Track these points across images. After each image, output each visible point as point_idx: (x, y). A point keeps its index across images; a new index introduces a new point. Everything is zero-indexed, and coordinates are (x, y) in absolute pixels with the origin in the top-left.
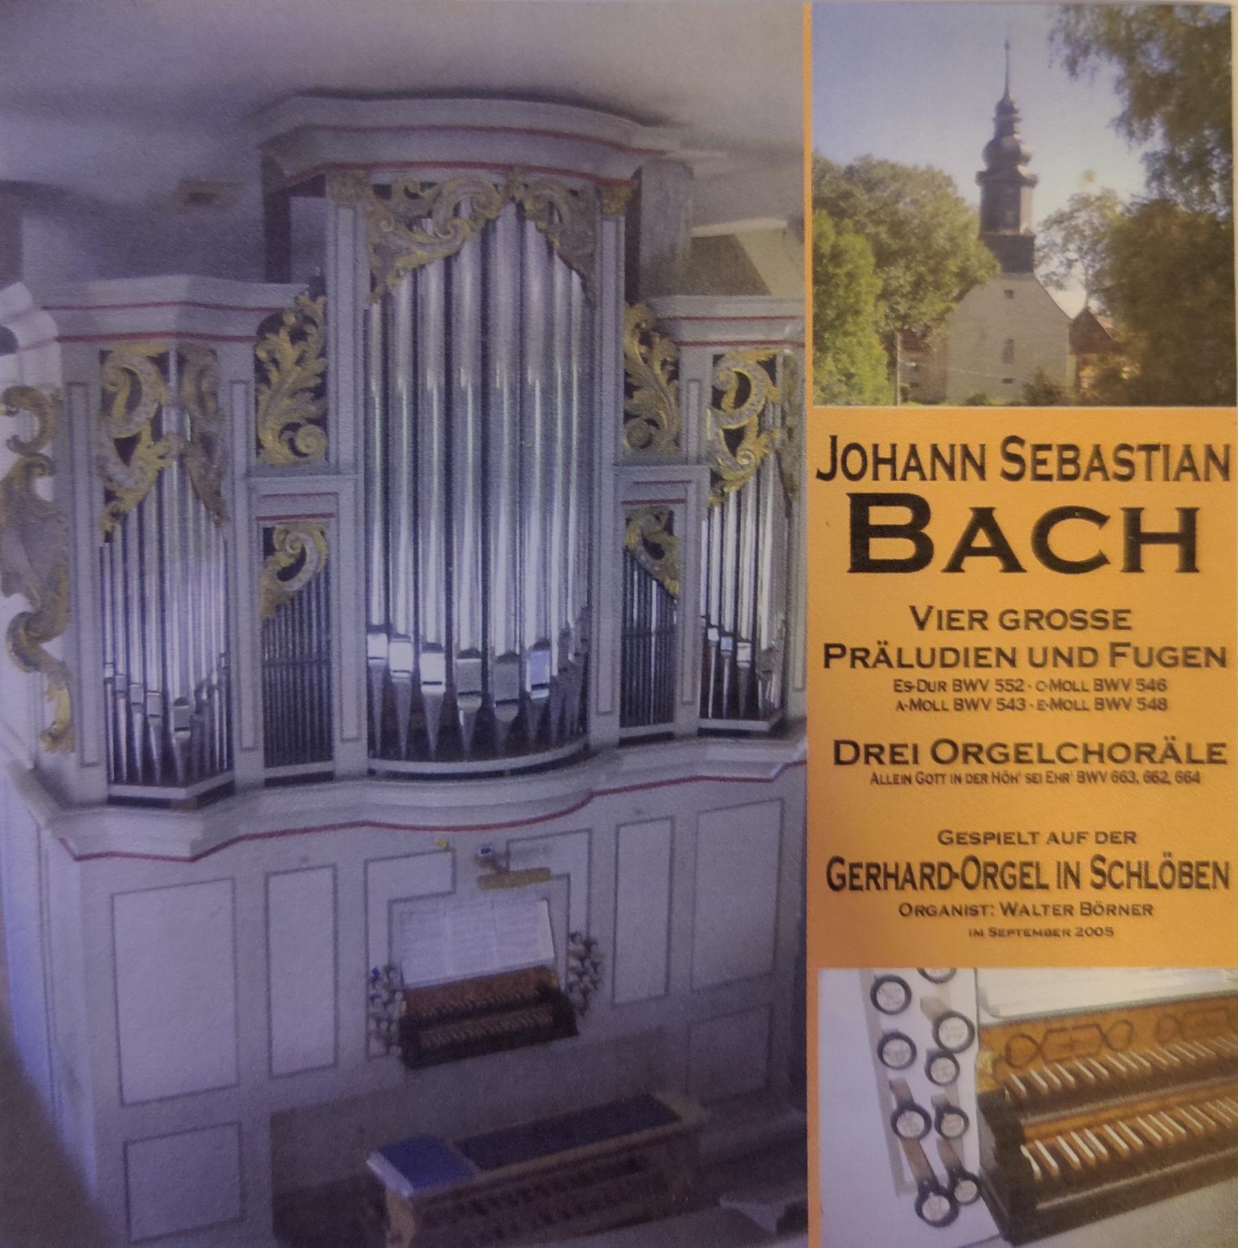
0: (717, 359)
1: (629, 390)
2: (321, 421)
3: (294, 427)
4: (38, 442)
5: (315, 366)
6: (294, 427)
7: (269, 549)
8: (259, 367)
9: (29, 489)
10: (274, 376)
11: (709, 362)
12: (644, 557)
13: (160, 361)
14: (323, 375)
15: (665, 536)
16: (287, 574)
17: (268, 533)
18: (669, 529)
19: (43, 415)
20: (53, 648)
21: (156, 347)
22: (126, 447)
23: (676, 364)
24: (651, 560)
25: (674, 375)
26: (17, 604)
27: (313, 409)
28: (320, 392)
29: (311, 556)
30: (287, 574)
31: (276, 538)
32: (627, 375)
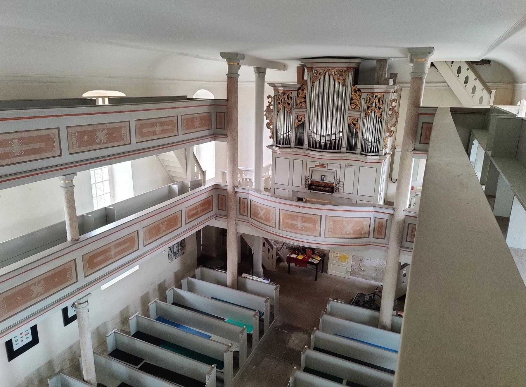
0: (367, 95)
1: (352, 100)
2: (305, 102)
3: (301, 102)
4: (271, 102)
5: (304, 95)
6: (301, 102)
7: (297, 118)
8: (297, 94)
9: (270, 108)
10: (299, 96)
11: (366, 95)
12: (352, 125)
13: (282, 93)
14: (305, 96)
15: (356, 122)
16: (299, 121)
17: (297, 116)
18: (357, 121)
19: (272, 99)
20: (271, 127)
21: (281, 91)
22: (279, 103)
23: (361, 95)
24: (353, 126)
25: (360, 97)
26: (268, 121)
27: (304, 100)
28: (305, 98)
29: (302, 119)
30: (299, 121)
31: (298, 116)
32: (351, 97)
